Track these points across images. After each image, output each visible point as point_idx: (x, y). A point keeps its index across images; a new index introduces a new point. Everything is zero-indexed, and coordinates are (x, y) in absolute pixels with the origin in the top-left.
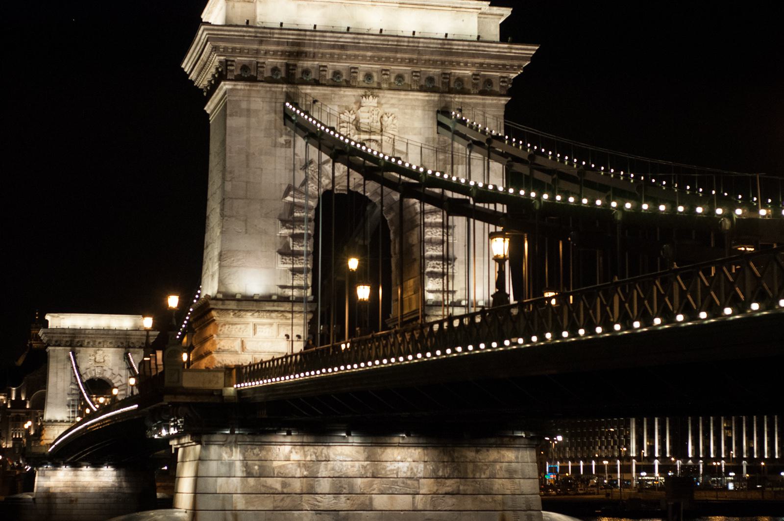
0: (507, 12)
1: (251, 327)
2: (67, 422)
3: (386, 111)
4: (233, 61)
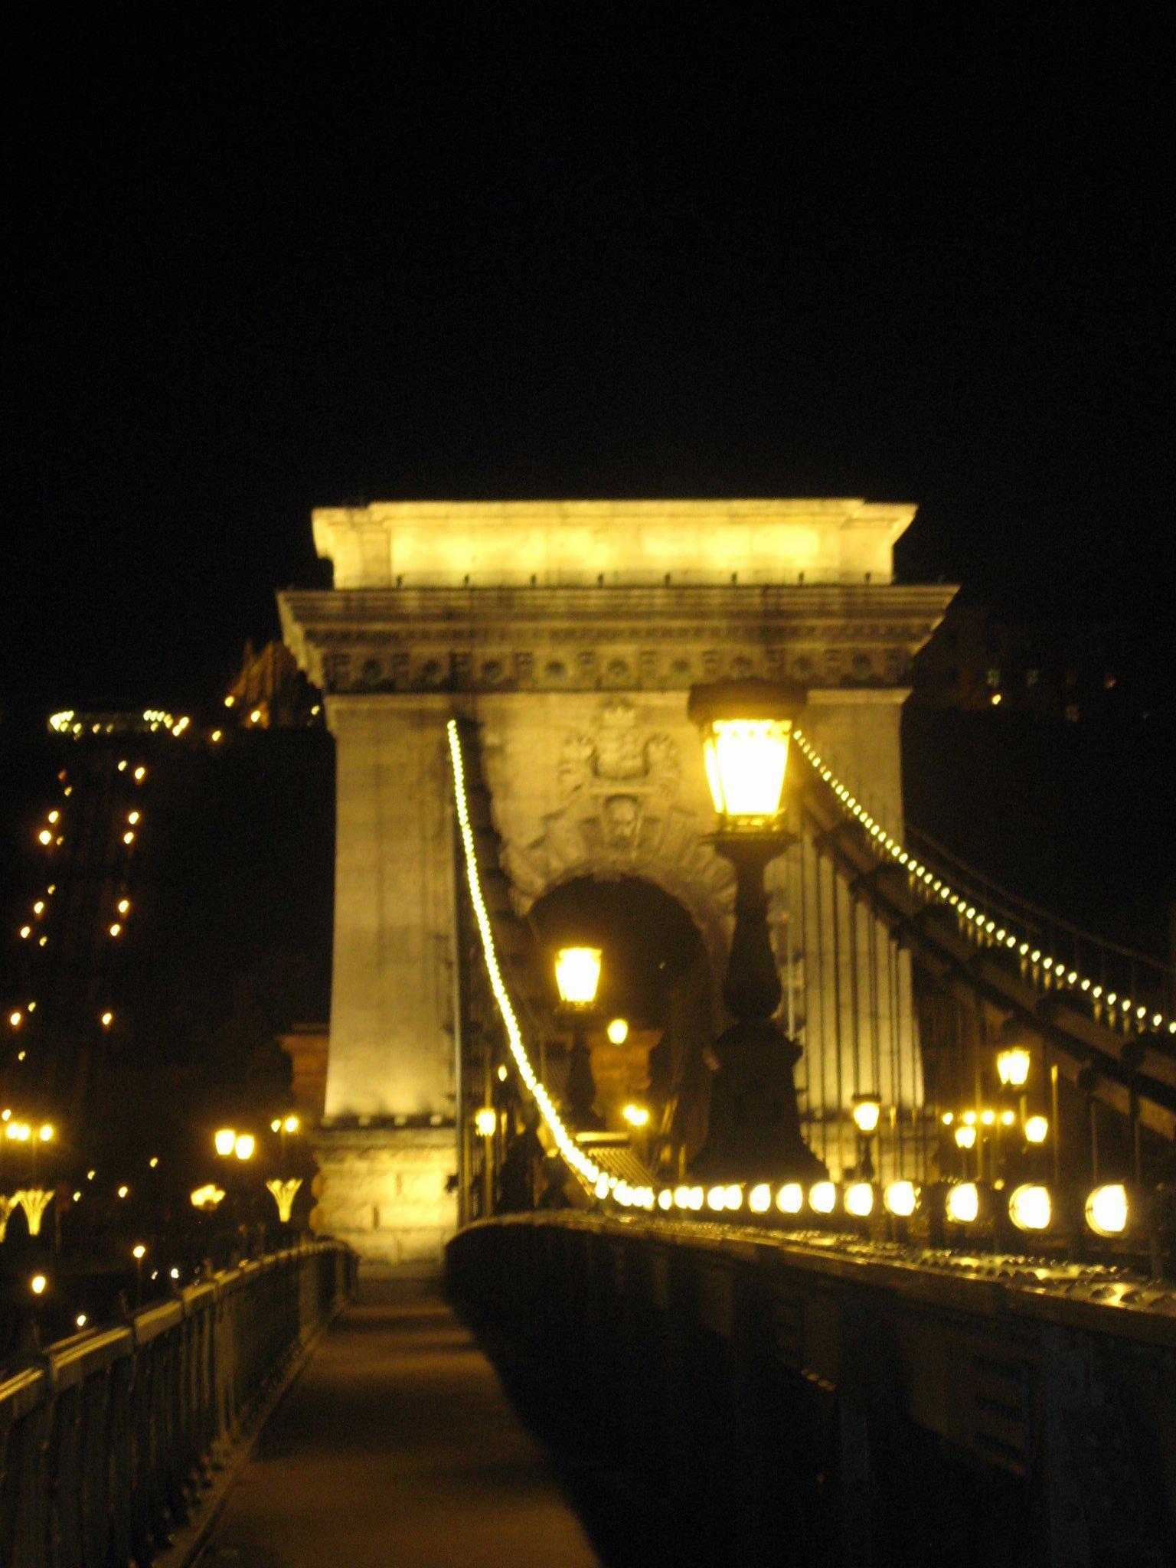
2: (447, 1123)
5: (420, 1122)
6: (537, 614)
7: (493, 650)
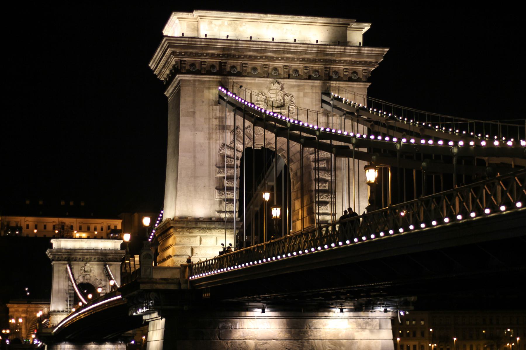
0: (366, 27)
1: (198, 239)
2: (66, 312)
3: (287, 92)
4: (185, 61)
5: (63, 311)
6: (78, 252)
7: (73, 256)
